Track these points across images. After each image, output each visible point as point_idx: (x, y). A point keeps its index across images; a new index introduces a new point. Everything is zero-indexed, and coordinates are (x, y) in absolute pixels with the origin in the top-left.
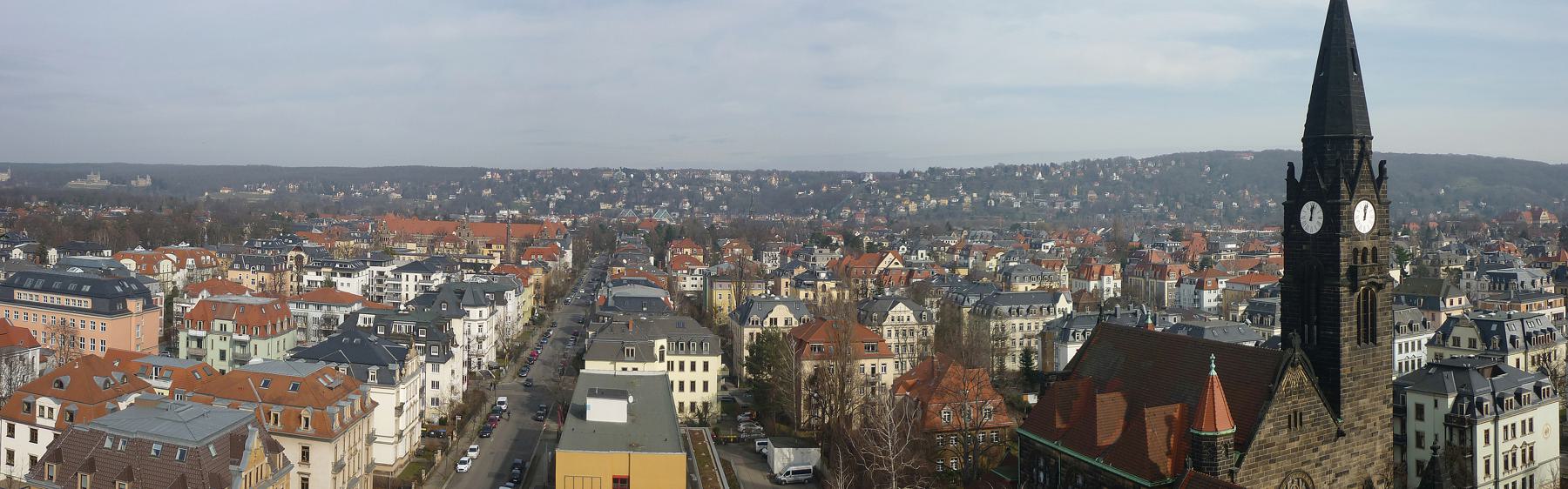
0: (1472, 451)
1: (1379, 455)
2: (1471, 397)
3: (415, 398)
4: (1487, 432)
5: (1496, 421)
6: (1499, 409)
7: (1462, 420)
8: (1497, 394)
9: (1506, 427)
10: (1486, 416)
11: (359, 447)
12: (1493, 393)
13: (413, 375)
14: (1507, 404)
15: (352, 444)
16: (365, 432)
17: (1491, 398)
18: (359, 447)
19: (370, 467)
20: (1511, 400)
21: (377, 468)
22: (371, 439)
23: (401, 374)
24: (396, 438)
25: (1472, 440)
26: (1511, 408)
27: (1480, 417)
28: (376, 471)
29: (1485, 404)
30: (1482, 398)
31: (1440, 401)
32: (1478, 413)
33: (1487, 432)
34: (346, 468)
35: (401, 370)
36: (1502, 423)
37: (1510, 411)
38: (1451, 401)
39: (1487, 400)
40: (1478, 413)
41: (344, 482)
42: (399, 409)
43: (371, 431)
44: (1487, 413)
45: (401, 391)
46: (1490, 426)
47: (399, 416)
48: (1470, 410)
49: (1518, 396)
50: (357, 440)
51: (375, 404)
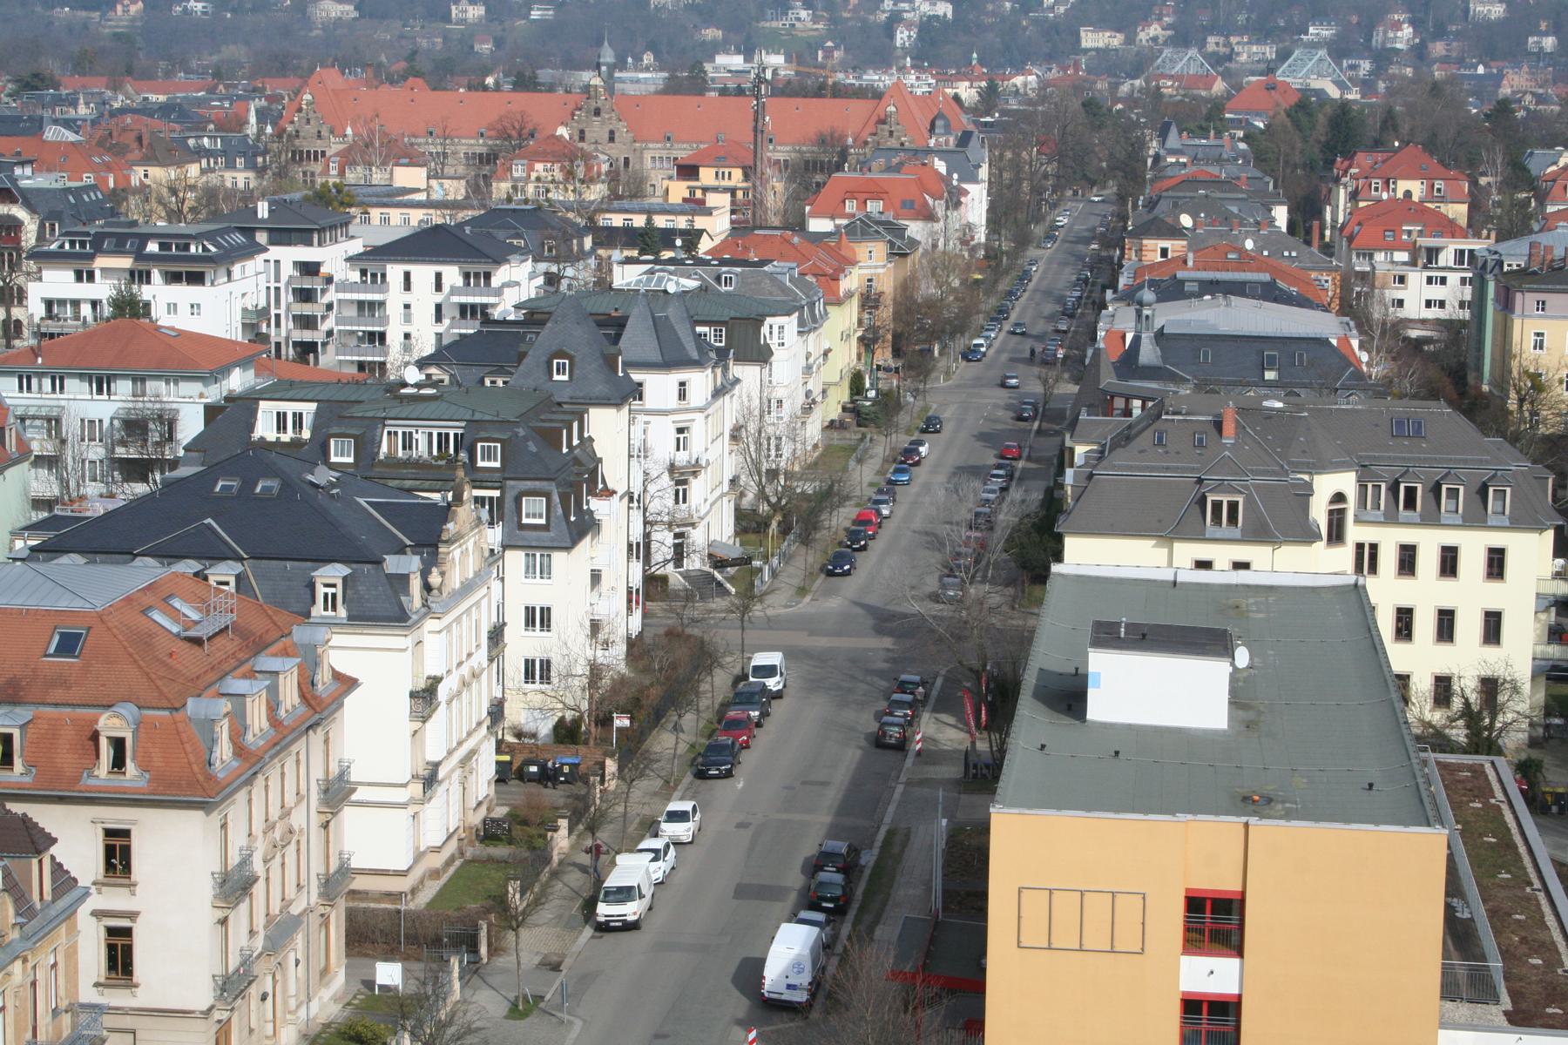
3: (474, 662)
11: (298, 819)
13: (468, 588)
15: (275, 813)
16: (317, 773)
18: (298, 819)
19: (336, 881)
21: (359, 883)
22: (337, 793)
23: (427, 588)
24: (417, 789)
28: (353, 894)
34: (259, 889)
35: (425, 574)
41: (252, 933)
42: (425, 697)
43: (334, 770)
45: (429, 640)
47: (425, 720)
50: (290, 799)
51: (347, 684)
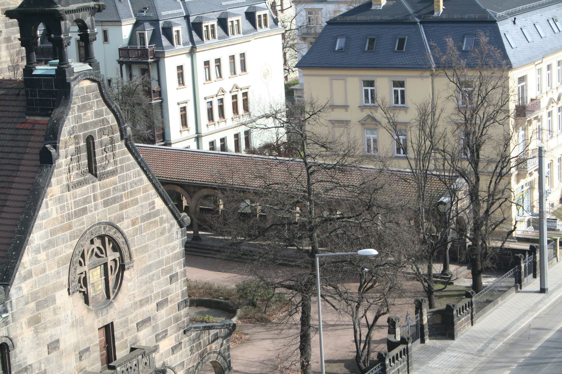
0: (160, 94)
1: (5, 66)
2: (155, 22)
4: (180, 68)
5: (192, 52)
6: (196, 38)
7: (144, 53)
8: (192, 19)
9: (207, 63)
10: (177, 47)
12: (187, 17)
14: (207, 31)
17: (184, 23)
20: (213, 26)
25: (159, 81)
26: (214, 37)
27: (168, 48)
29: (175, 29)
30: (170, 23)
31: (111, 31)
32: (165, 42)
33: (180, 68)
36: (201, 57)
37: (212, 41)
38: (126, 30)
39: (177, 25)
40: (165, 42)
44: (179, 43)
46: (185, 61)
48: (155, 38)
49: (222, 22)
